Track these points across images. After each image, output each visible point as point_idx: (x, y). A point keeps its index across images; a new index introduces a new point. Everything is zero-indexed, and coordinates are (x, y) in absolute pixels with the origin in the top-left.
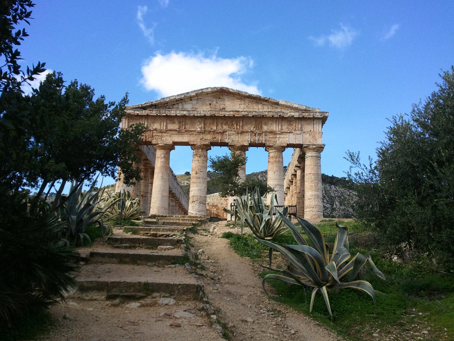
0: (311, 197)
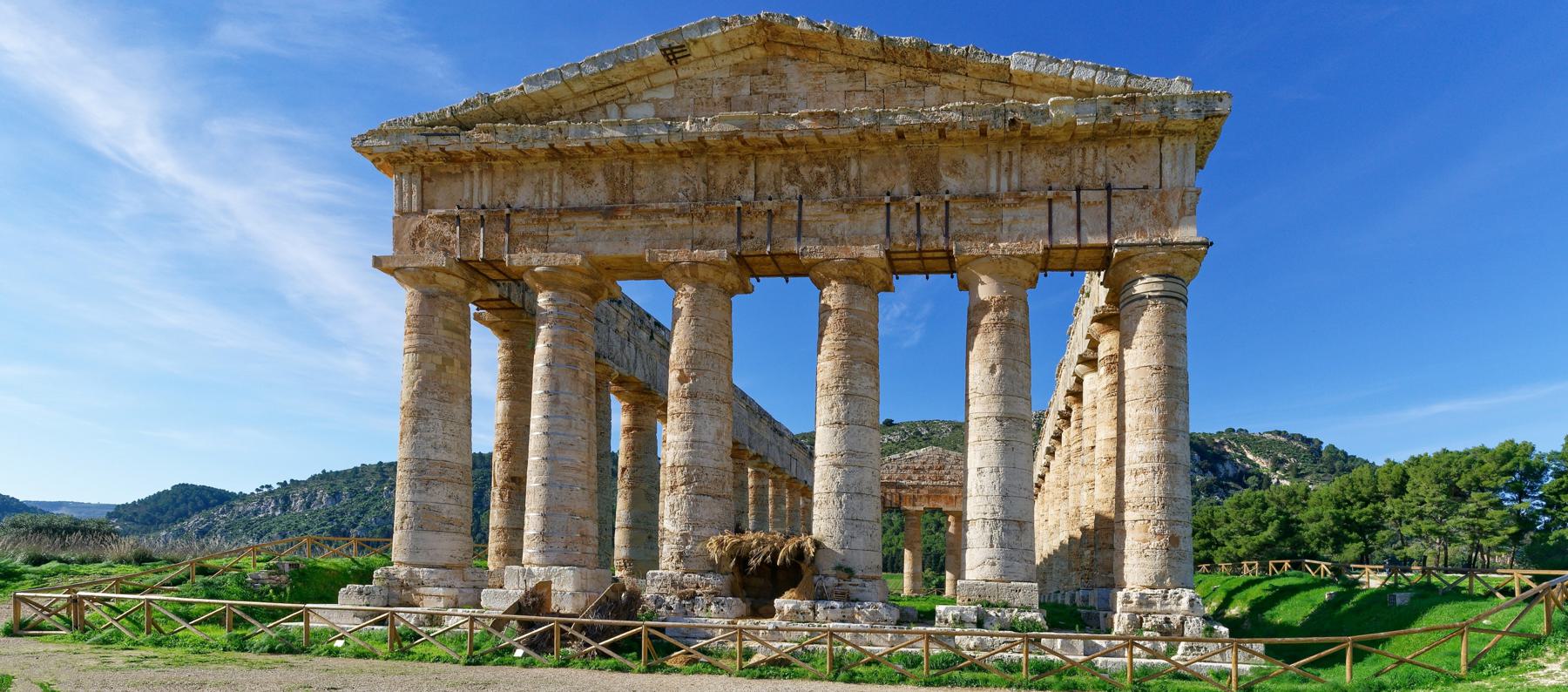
0: (1146, 465)
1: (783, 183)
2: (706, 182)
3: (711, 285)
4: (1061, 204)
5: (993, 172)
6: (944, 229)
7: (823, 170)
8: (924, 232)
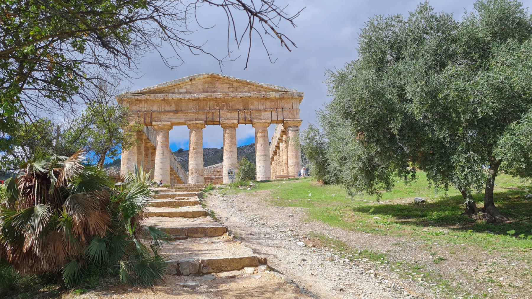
5: (260, 105)
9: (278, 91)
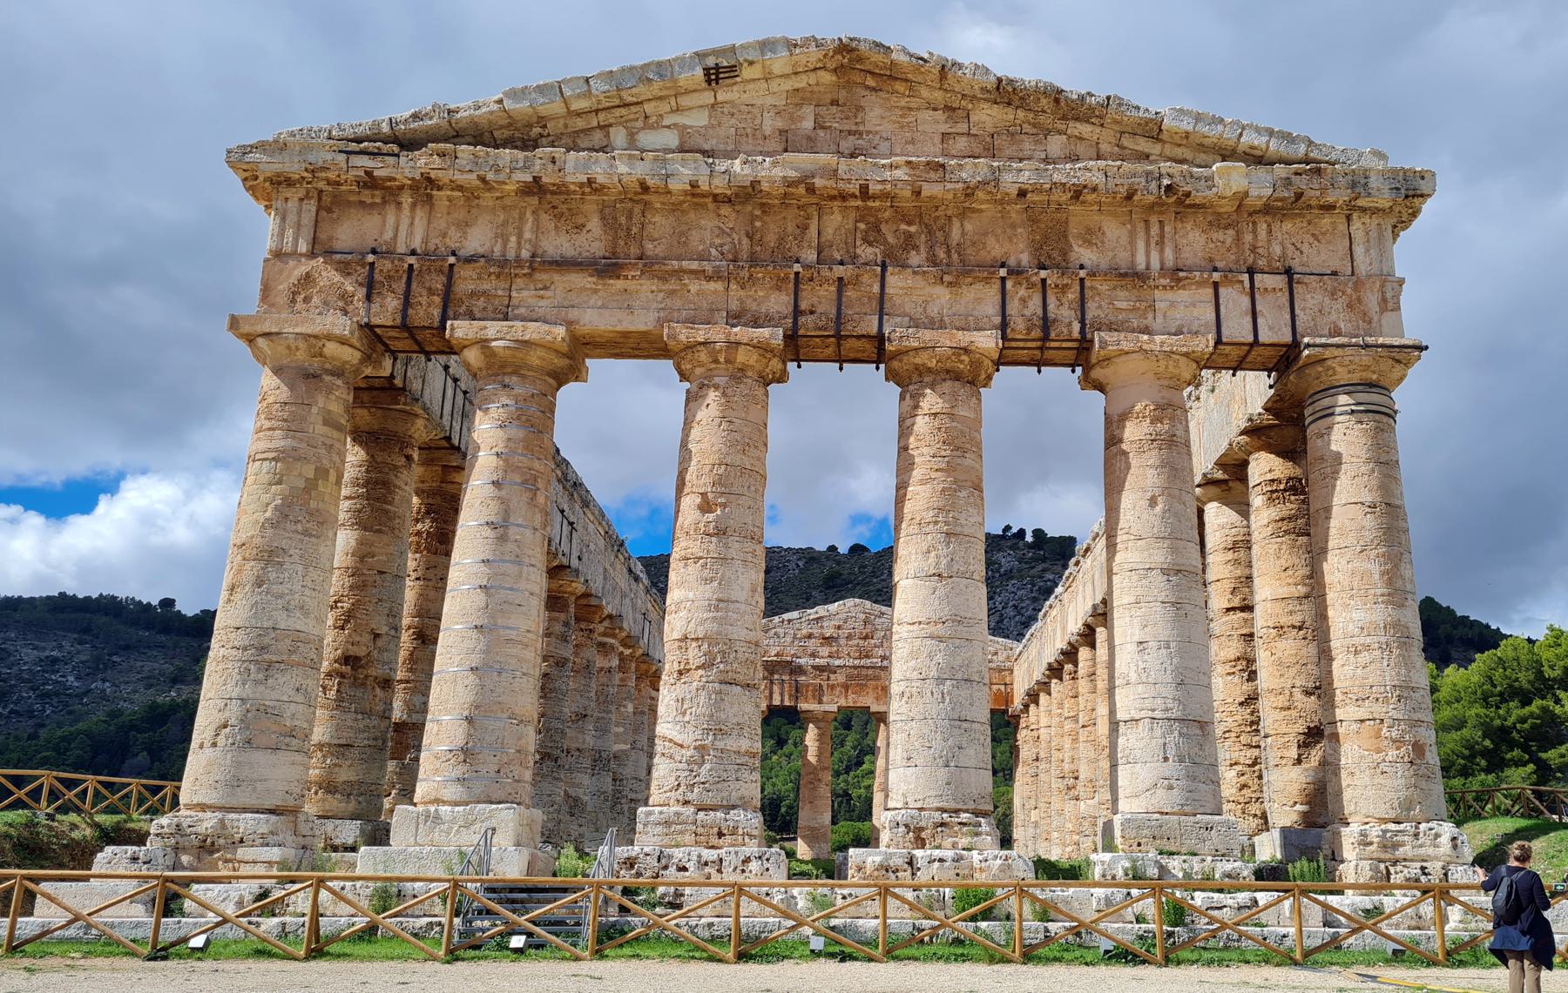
0: (1368, 640)
1: (858, 243)
2: (750, 236)
3: (750, 374)
4: (1230, 290)
5: (1141, 245)
6: (1079, 313)
7: (913, 229)
8: (1051, 315)
9: (1257, 159)
